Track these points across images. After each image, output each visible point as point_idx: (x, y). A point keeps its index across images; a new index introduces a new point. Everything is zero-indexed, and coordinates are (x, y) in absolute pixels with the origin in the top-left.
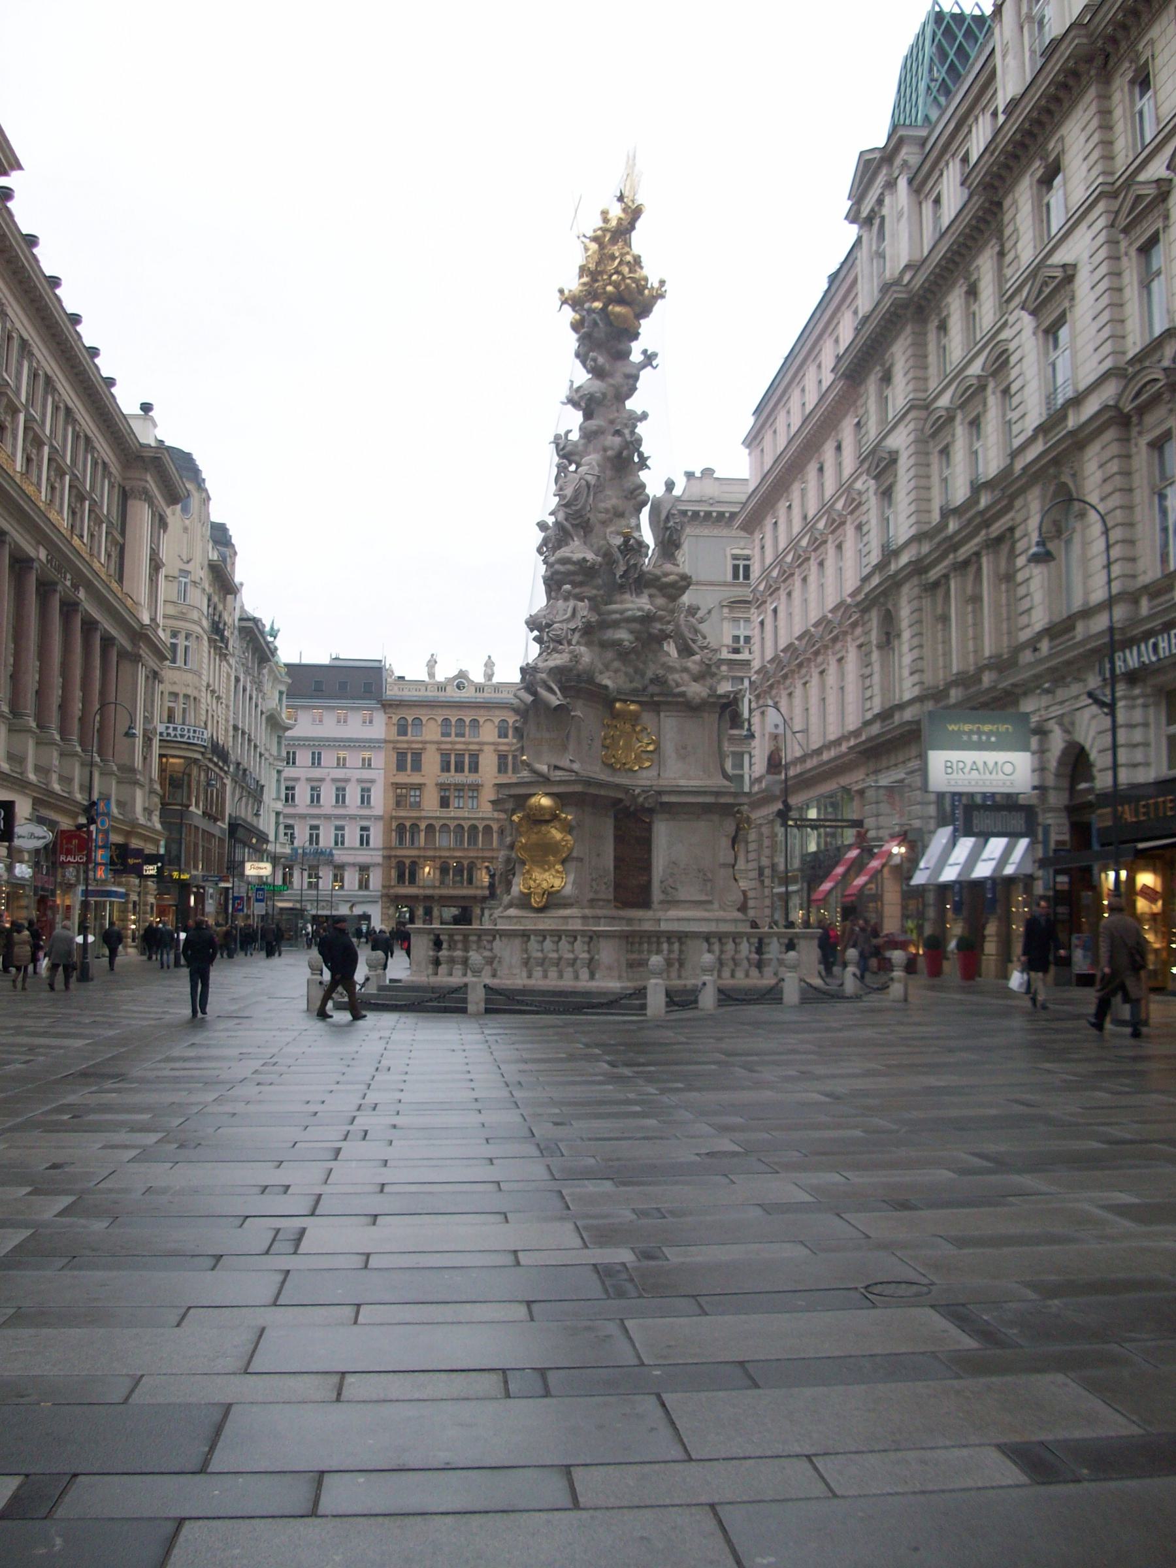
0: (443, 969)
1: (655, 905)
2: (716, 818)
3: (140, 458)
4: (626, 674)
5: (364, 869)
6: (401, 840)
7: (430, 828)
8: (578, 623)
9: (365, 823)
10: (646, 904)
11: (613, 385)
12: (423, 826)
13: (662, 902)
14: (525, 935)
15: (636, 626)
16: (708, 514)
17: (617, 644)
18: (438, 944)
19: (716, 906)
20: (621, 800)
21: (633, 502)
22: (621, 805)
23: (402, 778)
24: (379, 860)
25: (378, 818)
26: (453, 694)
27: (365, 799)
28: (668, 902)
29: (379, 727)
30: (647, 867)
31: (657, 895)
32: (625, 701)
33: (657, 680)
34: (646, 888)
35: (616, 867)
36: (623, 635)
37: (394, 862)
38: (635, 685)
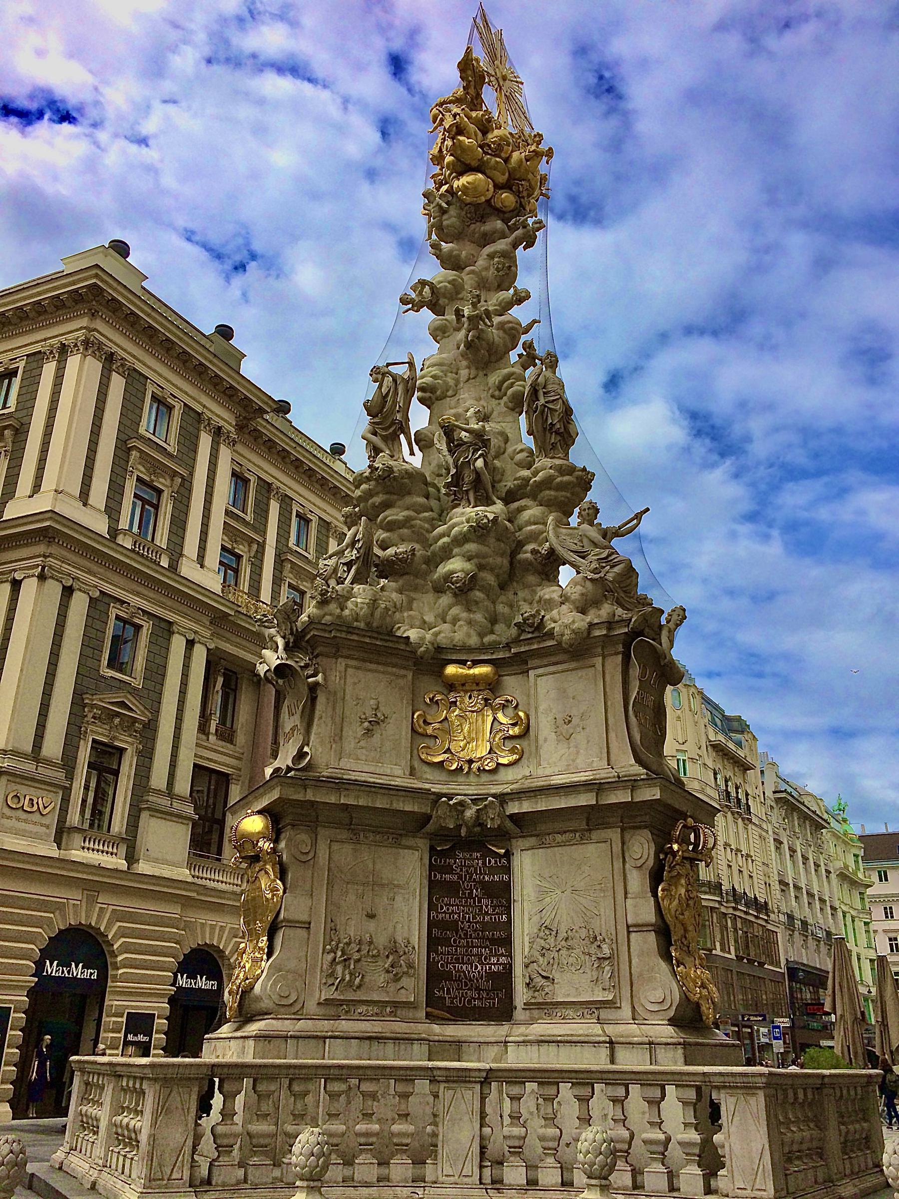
1: (519, 1014)
2: (615, 835)
4: (470, 623)
10: (503, 1012)
11: (472, 272)
13: (528, 1006)
15: (471, 547)
17: (448, 577)
19: (626, 1012)
21: (505, 398)
22: (430, 827)
28: (540, 1006)
30: (504, 942)
32: (463, 663)
34: (503, 980)
35: (433, 943)
36: (456, 565)
38: (486, 640)
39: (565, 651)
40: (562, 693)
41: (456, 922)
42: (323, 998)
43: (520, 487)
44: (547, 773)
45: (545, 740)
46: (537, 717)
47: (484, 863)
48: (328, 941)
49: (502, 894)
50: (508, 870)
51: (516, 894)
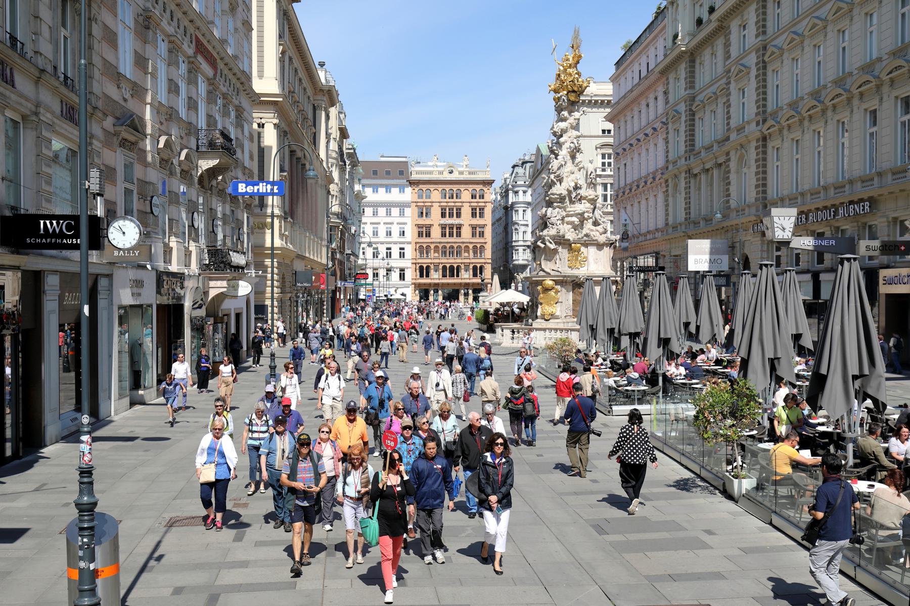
0: (515, 341)
3: (322, 90)
5: (402, 270)
6: (421, 253)
7: (436, 247)
8: (559, 217)
9: (402, 246)
12: (432, 246)
14: (544, 330)
16: (590, 101)
18: (513, 332)
23: (423, 221)
24: (410, 265)
25: (409, 243)
26: (447, 176)
27: (403, 233)
29: (409, 194)
33: (587, 235)
37: (418, 266)
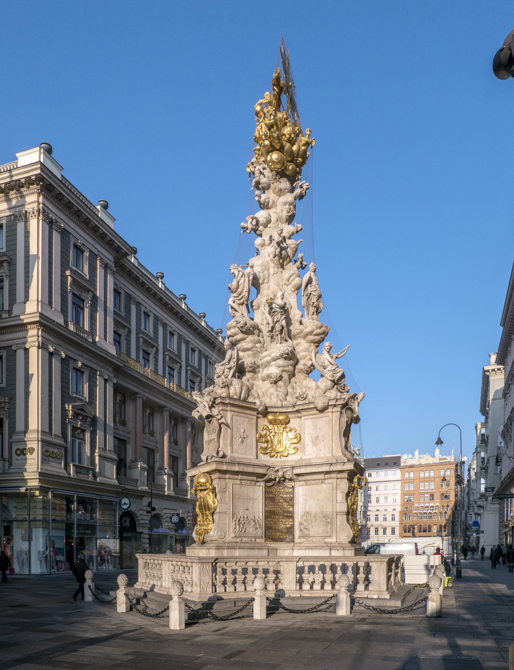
17: (269, 377)
20: (265, 475)
21: (290, 286)
31: (297, 533)
36: (273, 370)
39: (318, 410)
40: (315, 427)
41: (274, 511)
42: (233, 536)
43: (299, 333)
44: (309, 457)
45: (308, 445)
46: (304, 436)
47: (284, 491)
48: (233, 518)
49: (291, 501)
50: (293, 493)
51: (296, 501)
